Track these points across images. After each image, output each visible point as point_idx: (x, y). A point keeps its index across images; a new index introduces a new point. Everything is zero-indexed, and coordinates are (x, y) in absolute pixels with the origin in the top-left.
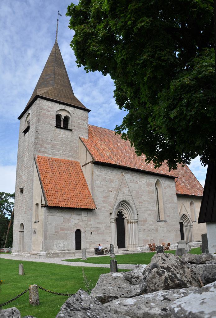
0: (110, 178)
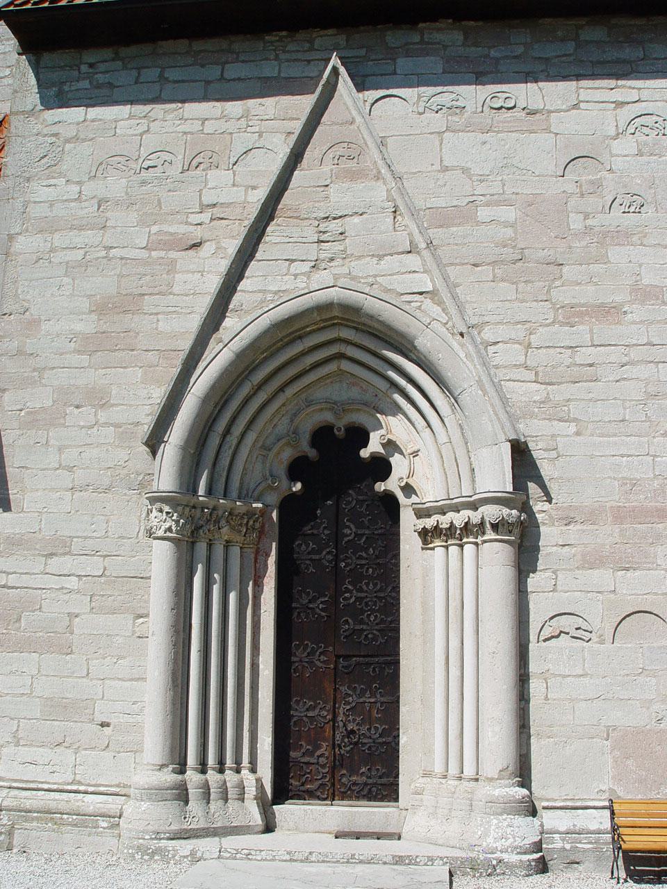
0: (197, 126)
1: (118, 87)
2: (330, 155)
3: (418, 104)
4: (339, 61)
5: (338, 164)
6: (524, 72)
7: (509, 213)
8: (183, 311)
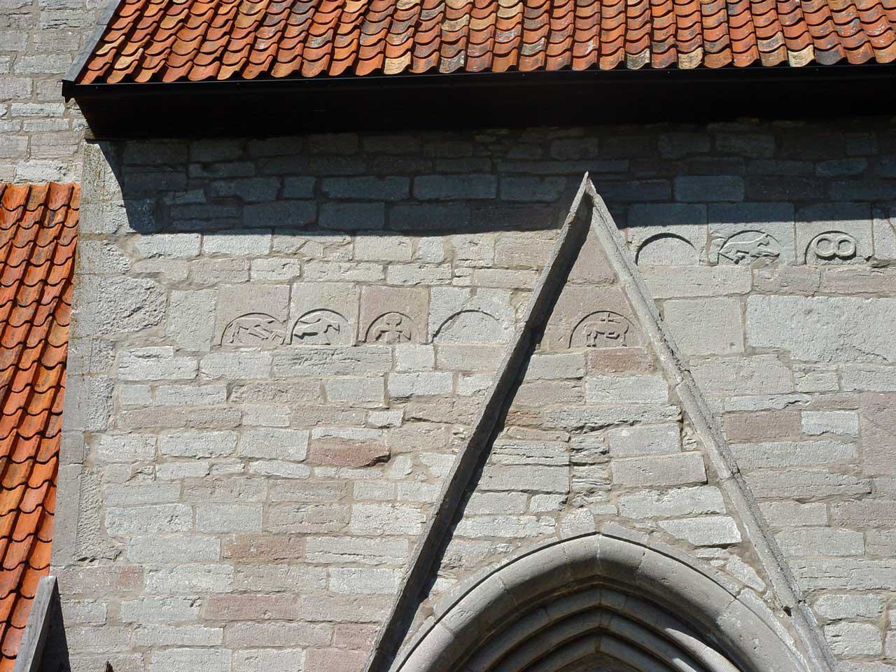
0: (375, 273)
1: (250, 203)
2: (583, 330)
3: (708, 249)
4: (593, 186)
5: (594, 346)
7: (850, 422)
8: (367, 561)
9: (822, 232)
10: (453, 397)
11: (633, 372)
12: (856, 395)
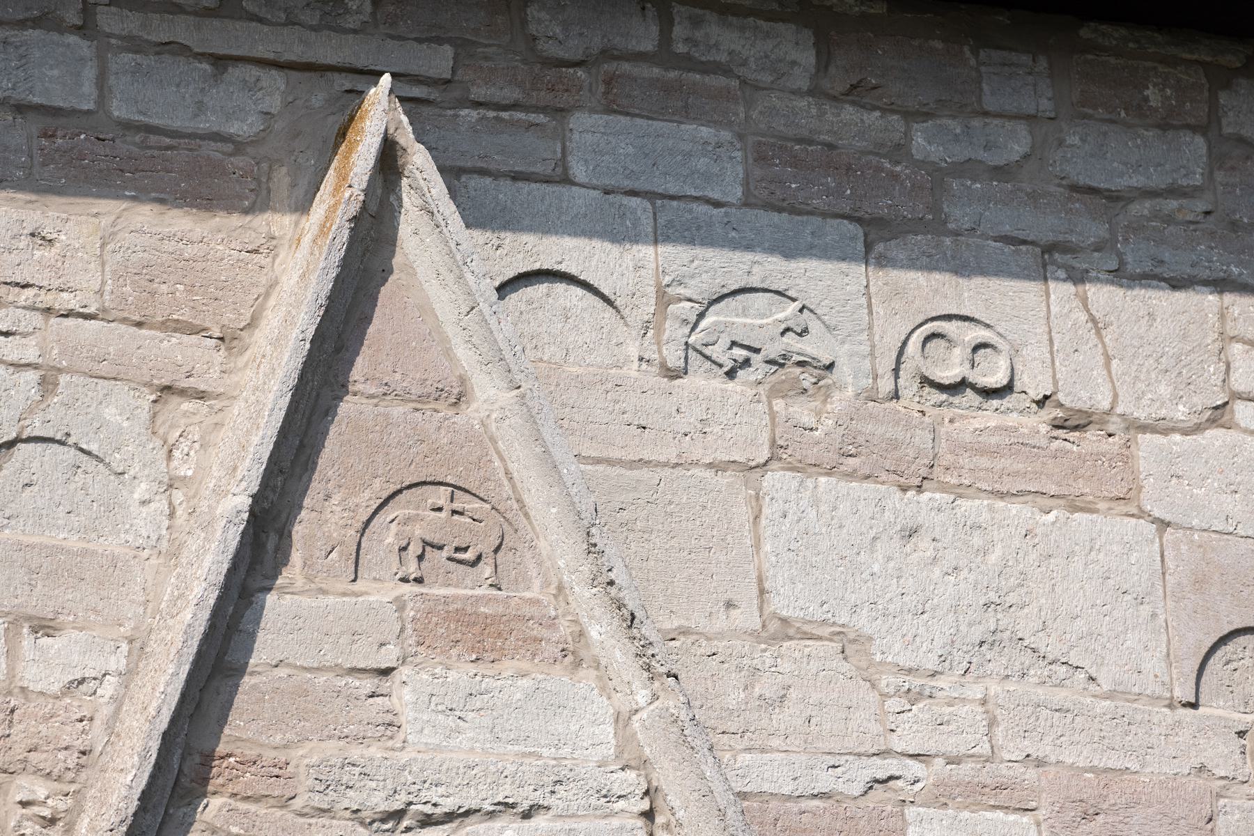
2: (387, 535)
4: (405, 119)
5: (419, 580)
6: (1032, 243)
9: (934, 314)
10: (10, 693)
11: (525, 665)
12: (1031, 774)
